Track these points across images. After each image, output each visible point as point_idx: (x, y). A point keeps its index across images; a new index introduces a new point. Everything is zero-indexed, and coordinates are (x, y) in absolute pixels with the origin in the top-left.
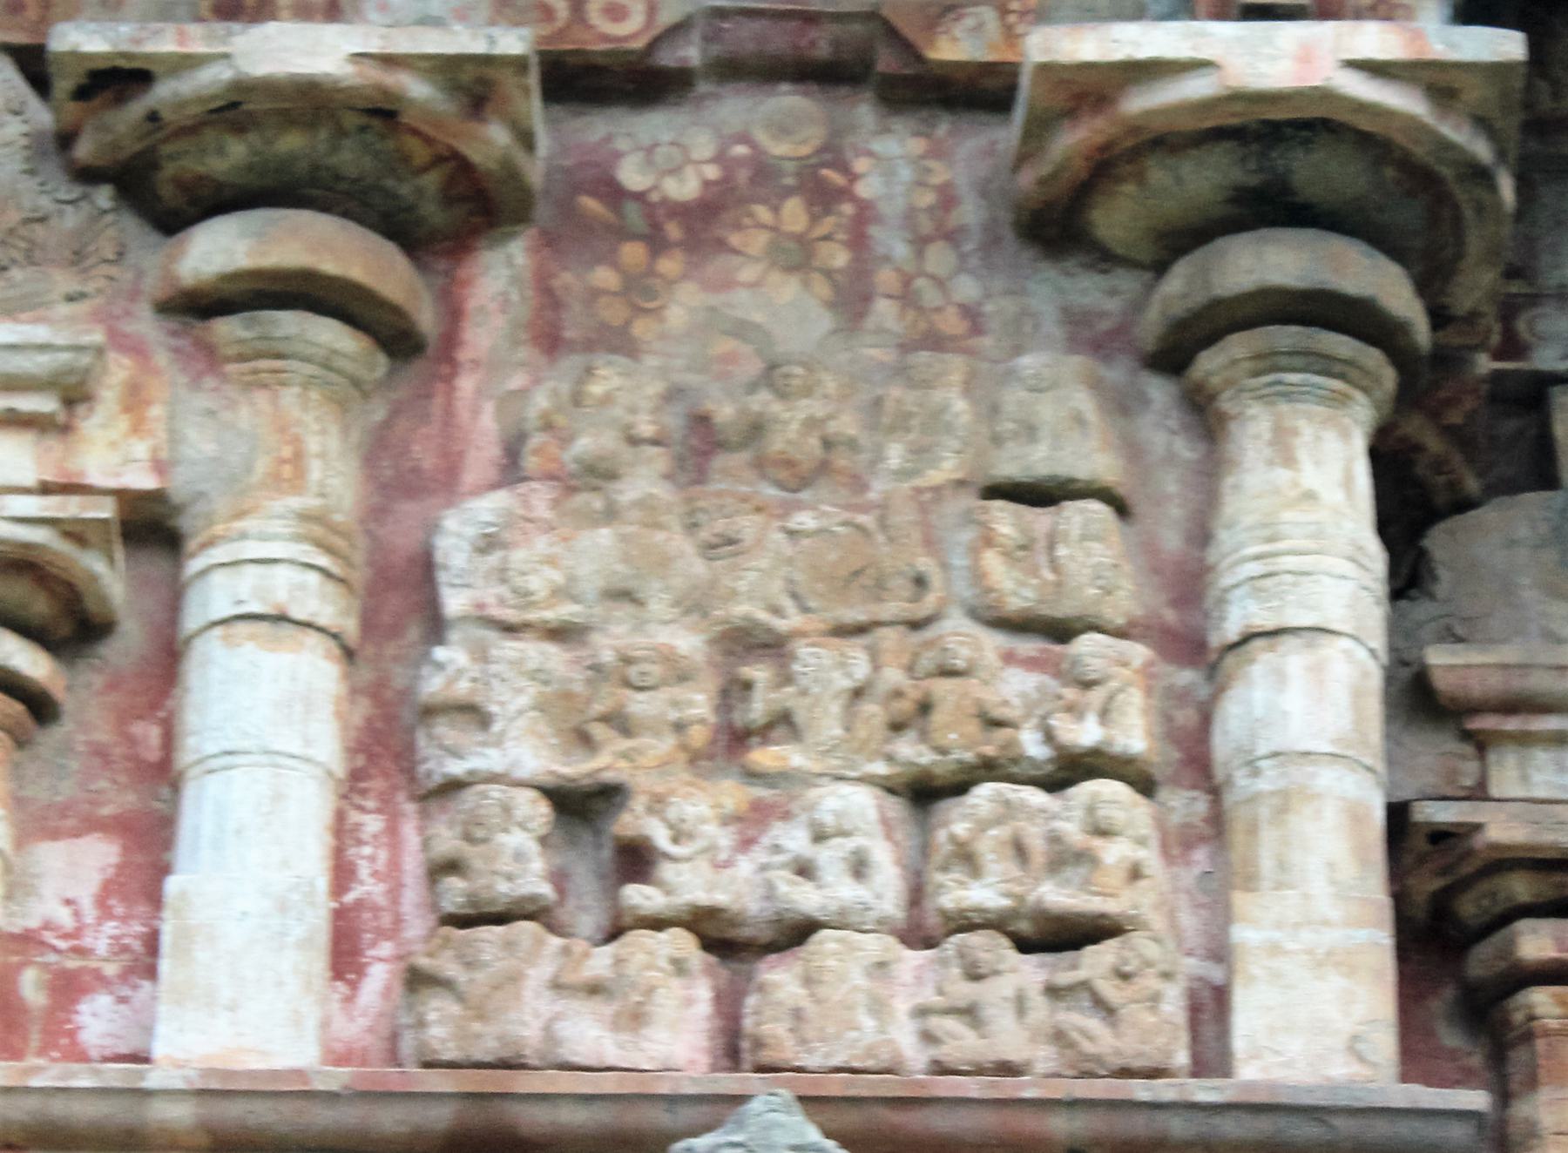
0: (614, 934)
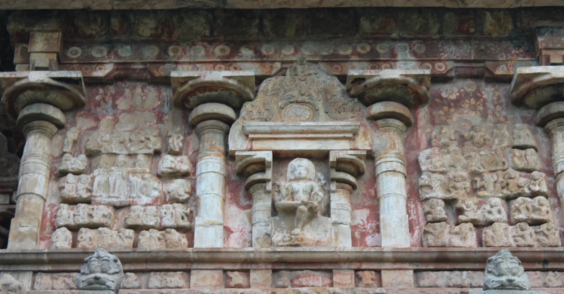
0: (457, 224)
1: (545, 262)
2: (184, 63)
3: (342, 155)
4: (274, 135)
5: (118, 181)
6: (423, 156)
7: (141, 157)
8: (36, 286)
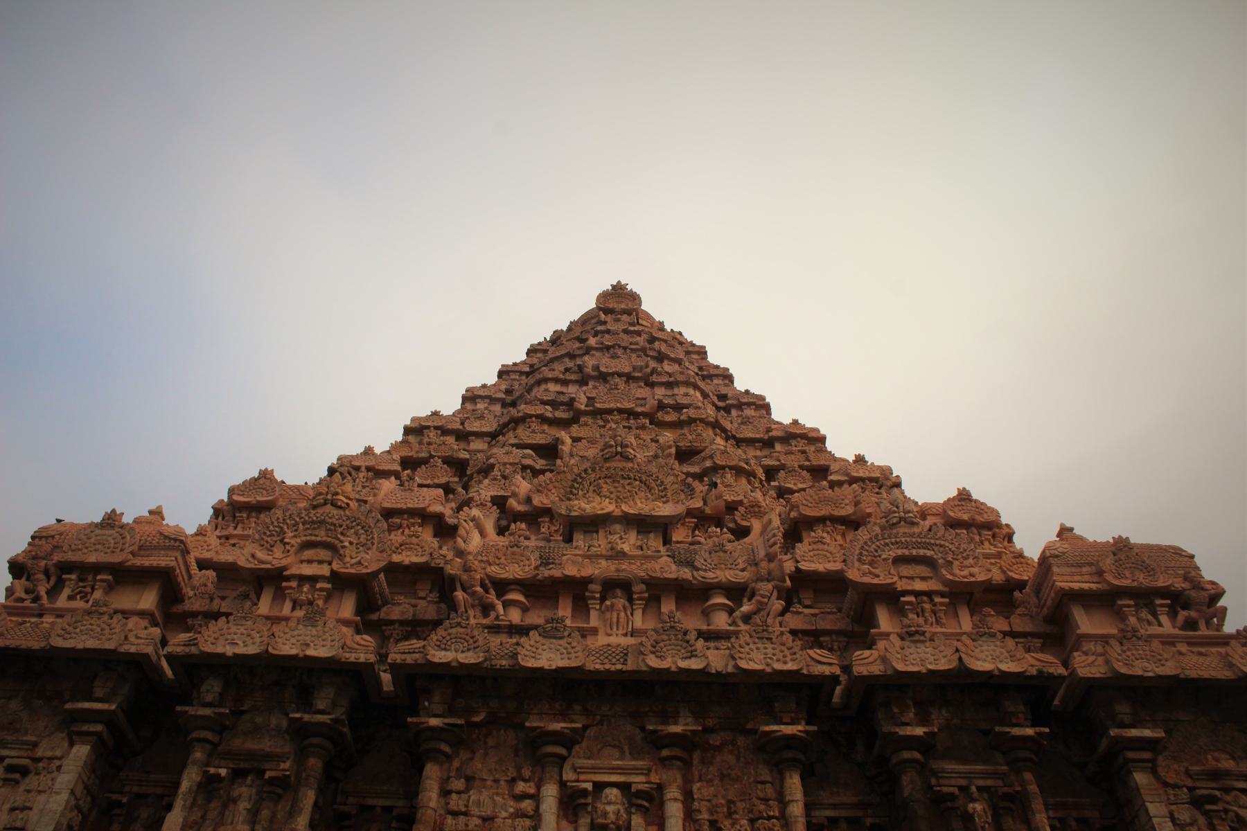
3: (641, 787)
4: (595, 770)
5: (486, 801)
6: (695, 787)
7: (502, 783)
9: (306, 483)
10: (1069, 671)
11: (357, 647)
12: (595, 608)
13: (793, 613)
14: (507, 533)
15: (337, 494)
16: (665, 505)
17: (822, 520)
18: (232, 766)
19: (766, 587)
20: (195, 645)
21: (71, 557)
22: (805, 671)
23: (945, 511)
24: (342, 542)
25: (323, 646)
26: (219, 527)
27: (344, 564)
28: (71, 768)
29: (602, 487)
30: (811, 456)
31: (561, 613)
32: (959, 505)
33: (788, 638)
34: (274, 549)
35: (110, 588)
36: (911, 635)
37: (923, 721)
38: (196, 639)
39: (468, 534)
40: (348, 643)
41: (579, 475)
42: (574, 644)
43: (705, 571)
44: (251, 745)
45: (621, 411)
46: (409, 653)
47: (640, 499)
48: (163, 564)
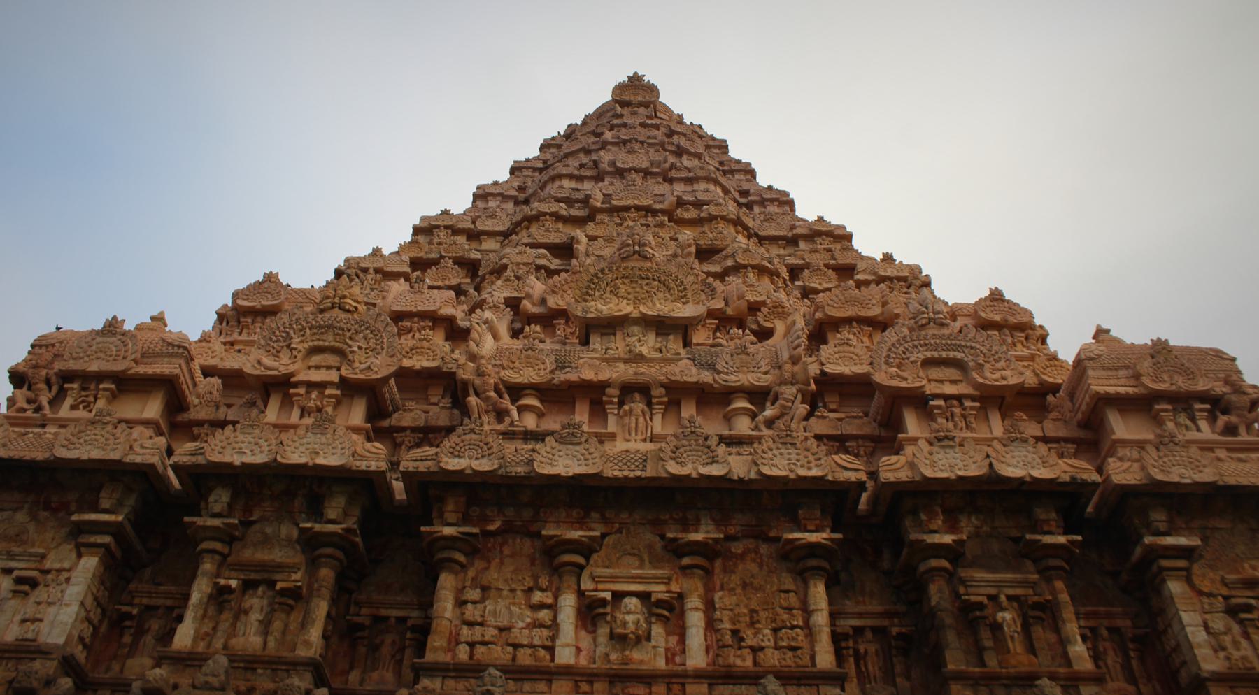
0: (740, 648)
1: (799, 679)
2: (550, 522)
3: (661, 596)
4: (614, 579)
5: (502, 611)
7: (519, 593)
8: (445, 688)
9: (312, 286)
10: (1103, 477)
11: (368, 455)
12: (612, 413)
13: (818, 417)
14: (521, 336)
15: (344, 297)
16: (685, 306)
17: (848, 321)
18: (242, 577)
19: (789, 391)
20: (201, 454)
21: (73, 365)
22: (830, 478)
23: (976, 312)
24: (350, 347)
25: (333, 454)
26: (224, 332)
27: (353, 369)
28: (80, 579)
29: (619, 288)
30: (837, 255)
31: (577, 418)
32: (991, 306)
33: (812, 443)
34: (281, 355)
35: (113, 397)
36: (942, 440)
37: (953, 529)
38: (203, 448)
39: (480, 337)
40: (359, 450)
41: (596, 275)
42: (592, 450)
43: (727, 374)
44: (262, 555)
45: (638, 208)
46: (422, 460)
47: (659, 300)
48: (167, 372)
